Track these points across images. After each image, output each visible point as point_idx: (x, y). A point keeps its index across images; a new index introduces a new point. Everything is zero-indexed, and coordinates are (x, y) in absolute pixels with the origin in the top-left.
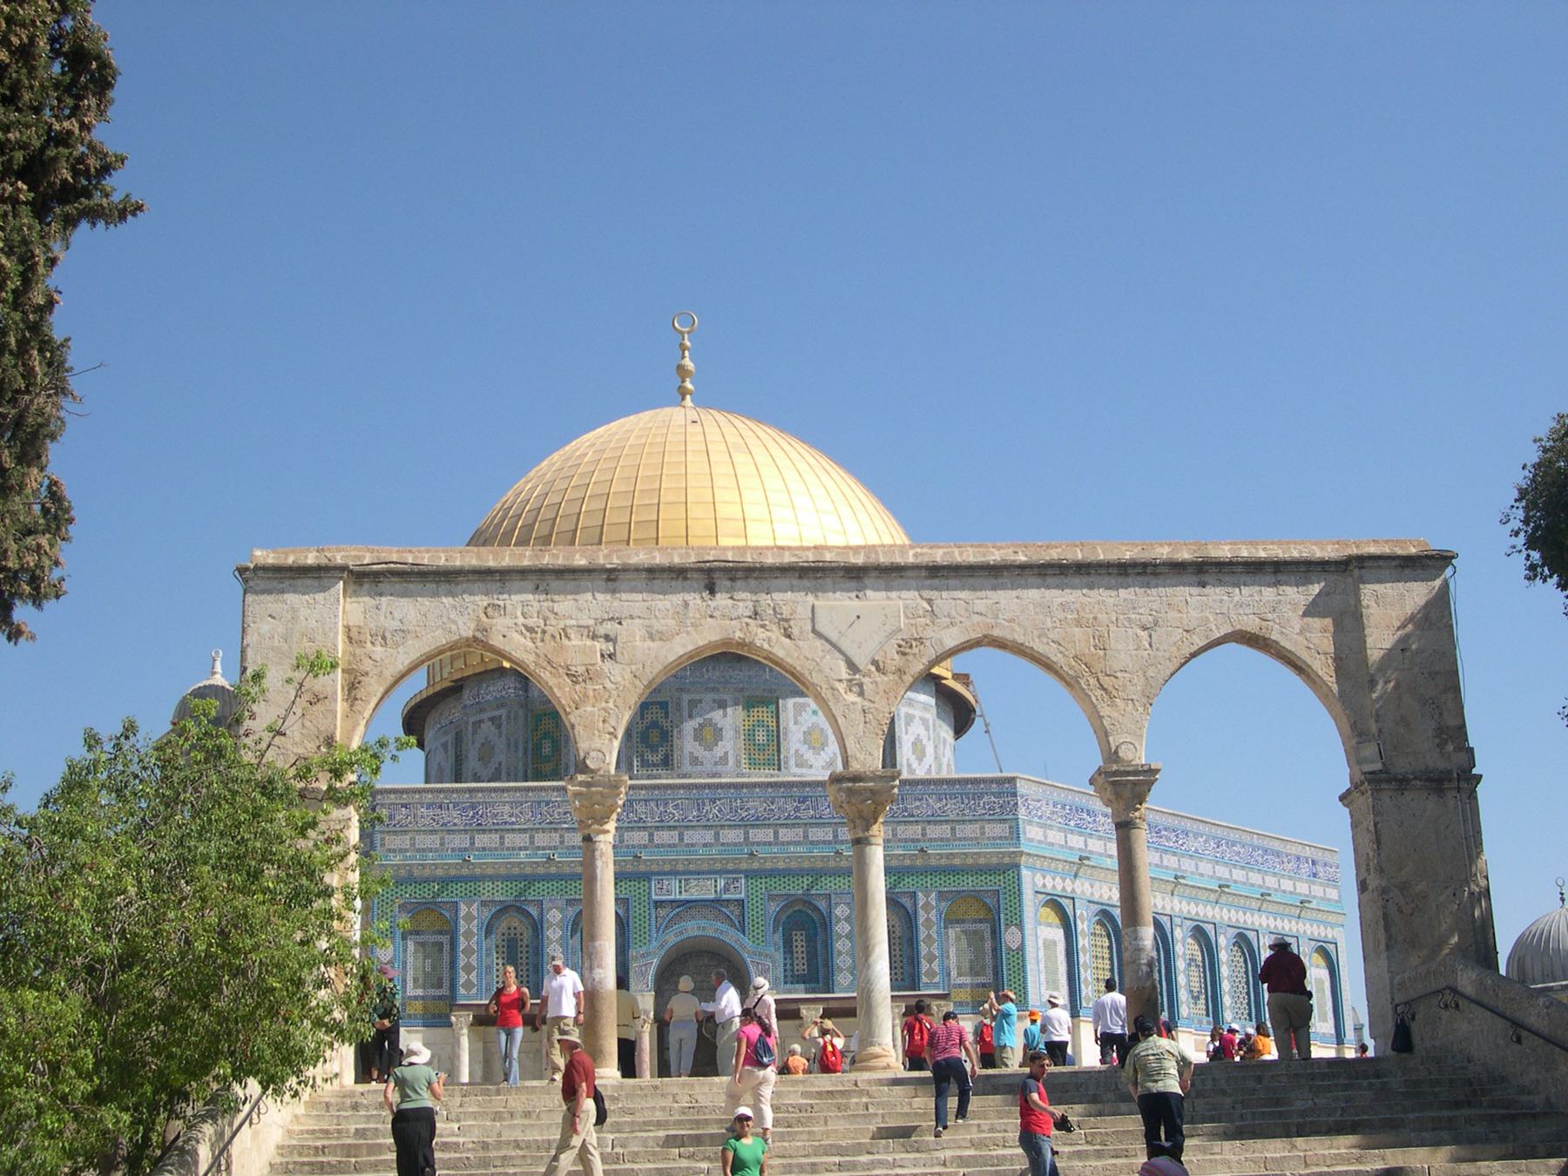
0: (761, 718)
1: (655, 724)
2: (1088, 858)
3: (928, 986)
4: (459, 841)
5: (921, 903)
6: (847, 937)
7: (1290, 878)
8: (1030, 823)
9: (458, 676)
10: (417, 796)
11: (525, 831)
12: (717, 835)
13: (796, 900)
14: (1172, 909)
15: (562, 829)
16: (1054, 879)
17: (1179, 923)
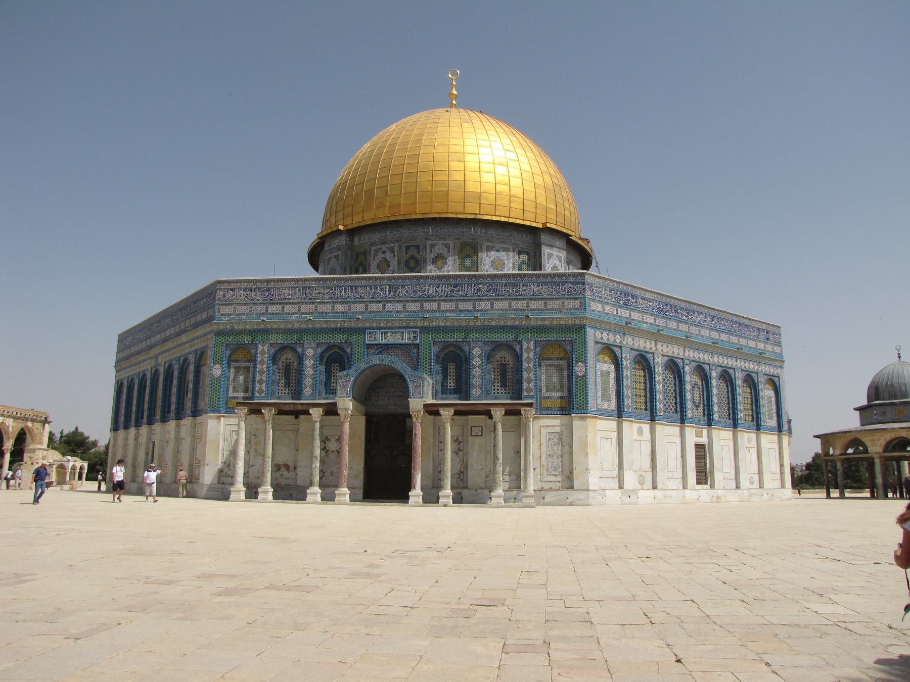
0: (468, 253)
1: (412, 257)
2: (630, 323)
3: (527, 397)
4: (260, 309)
5: (524, 347)
6: (479, 367)
7: (754, 340)
8: (593, 300)
9: (320, 236)
10: (239, 284)
11: (296, 303)
12: (405, 306)
13: (449, 345)
14: (684, 355)
15: (317, 302)
16: (608, 335)
17: (688, 363)
